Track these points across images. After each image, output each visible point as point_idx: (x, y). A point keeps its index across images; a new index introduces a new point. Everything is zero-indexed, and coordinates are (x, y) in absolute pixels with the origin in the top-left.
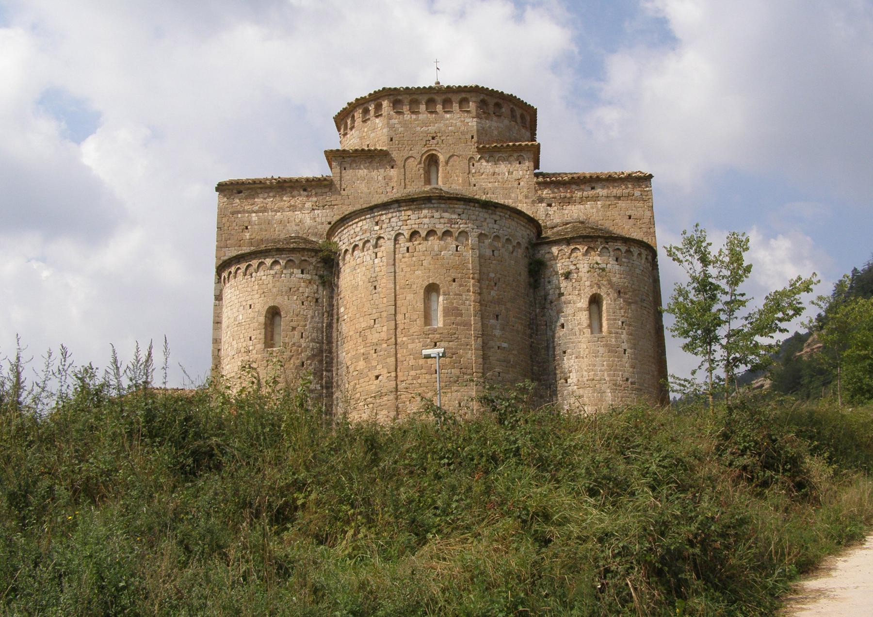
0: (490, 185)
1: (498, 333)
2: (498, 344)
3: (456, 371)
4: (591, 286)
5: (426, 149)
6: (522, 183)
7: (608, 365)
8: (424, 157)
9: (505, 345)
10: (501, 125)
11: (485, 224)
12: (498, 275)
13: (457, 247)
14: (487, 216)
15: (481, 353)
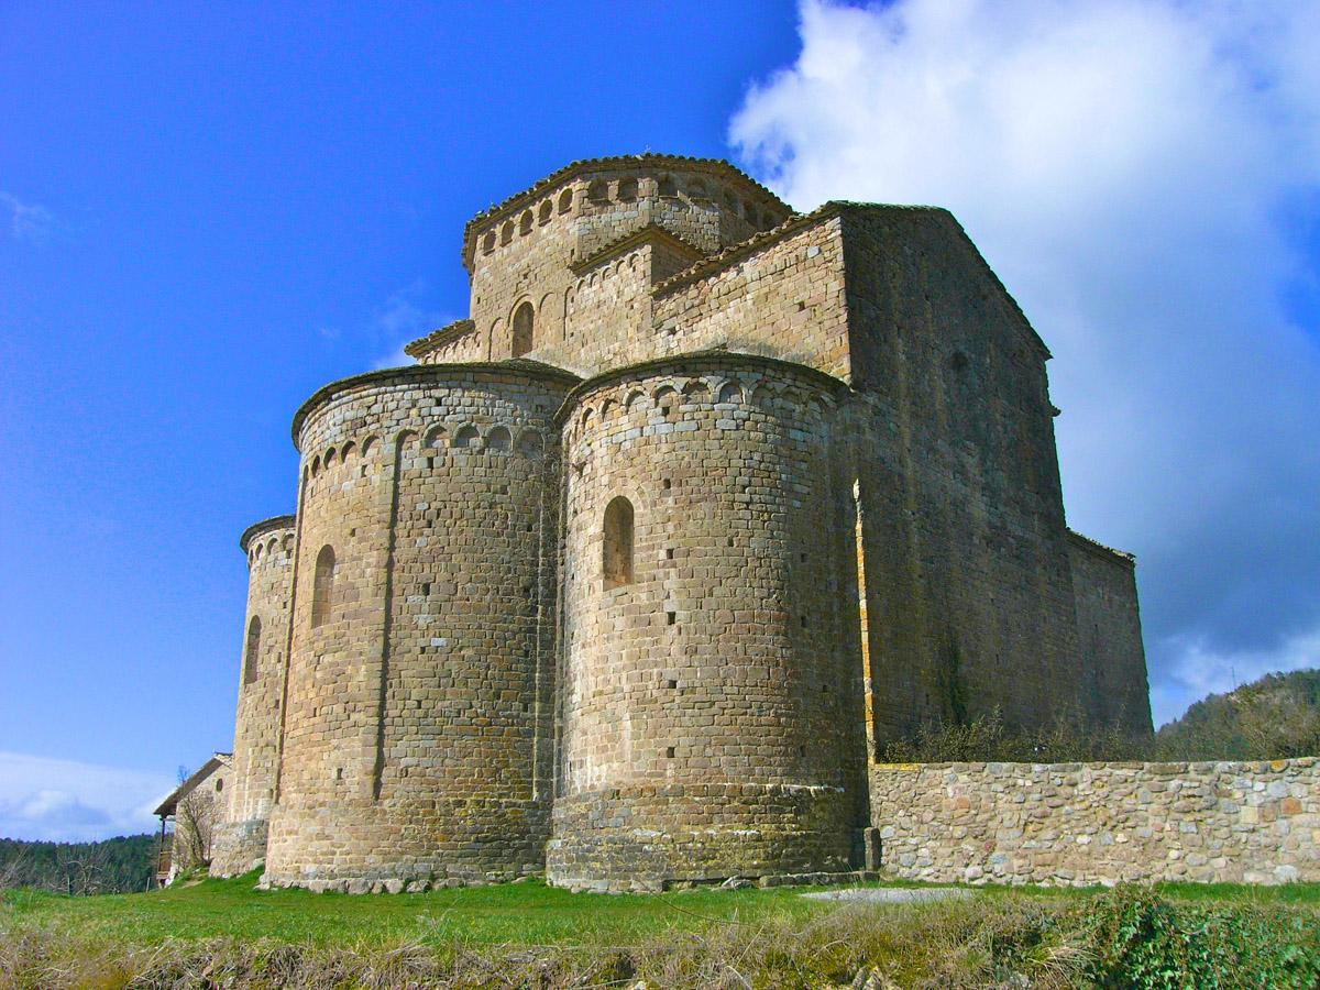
0: (592, 326)
1: (423, 620)
2: (422, 642)
4: (610, 485)
5: (516, 298)
6: (635, 306)
7: (630, 656)
9: (440, 641)
11: (414, 412)
13: (364, 467)
14: (418, 394)
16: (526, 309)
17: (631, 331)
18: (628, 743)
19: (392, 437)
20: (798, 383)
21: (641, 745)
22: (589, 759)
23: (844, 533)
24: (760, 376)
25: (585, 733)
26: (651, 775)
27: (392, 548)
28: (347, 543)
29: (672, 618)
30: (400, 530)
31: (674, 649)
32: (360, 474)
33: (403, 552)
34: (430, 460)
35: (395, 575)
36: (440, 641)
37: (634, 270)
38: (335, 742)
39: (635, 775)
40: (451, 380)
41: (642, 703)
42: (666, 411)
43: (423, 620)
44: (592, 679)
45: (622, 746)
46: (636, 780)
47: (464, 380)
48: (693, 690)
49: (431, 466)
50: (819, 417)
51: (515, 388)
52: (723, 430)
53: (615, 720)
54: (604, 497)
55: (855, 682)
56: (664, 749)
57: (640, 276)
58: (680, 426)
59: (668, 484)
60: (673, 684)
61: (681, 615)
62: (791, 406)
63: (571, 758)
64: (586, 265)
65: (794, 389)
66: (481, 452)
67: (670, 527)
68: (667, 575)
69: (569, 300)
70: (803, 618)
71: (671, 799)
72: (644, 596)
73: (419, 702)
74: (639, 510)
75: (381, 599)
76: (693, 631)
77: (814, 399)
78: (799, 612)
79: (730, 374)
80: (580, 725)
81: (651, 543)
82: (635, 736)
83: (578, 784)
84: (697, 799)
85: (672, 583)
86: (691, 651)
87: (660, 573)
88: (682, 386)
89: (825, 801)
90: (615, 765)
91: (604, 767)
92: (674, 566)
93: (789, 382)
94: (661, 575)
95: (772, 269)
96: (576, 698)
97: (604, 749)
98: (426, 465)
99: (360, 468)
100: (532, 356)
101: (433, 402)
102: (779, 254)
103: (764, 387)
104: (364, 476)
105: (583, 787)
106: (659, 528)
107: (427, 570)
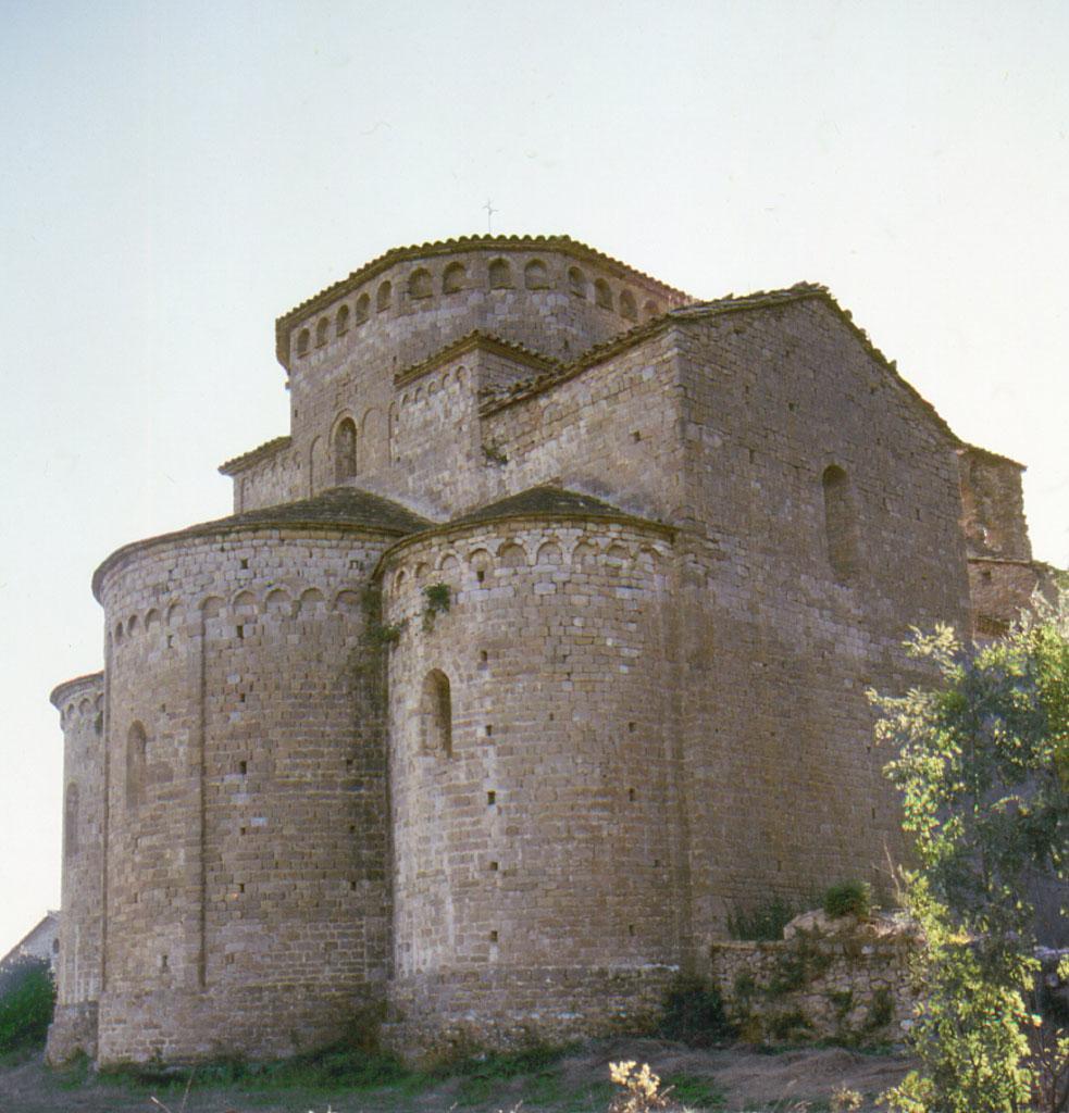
1: (241, 800)
2: (242, 823)
3: (159, 894)
4: (427, 658)
7: (451, 837)
8: (335, 430)
9: (261, 822)
10: (463, 311)
12: (249, 678)
13: (170, 637)
15: (196, 850)
16: (348, 424)
17: (461, 459)
18: (451, 927)
19: (197, 604)
20: (625, 536)
21: (463, 929)
22: (416, 941)
23: (681, 696)
24: (579, 532)
25: (410, 915)
26: (474, 960)
27: (204, 724)
28: (157, 720)
29: (492, 795)
30: (214, 703)
31: (494, 830)
32: (166, 645)
33: (216, 728)
34: (240, 629)
35: (209, 754)
36: (261, 822)
37: (461, 386)
38: (158, 929)
39: (459, 959)
40: (255, 538)
41: (464, 888)
42: (481, 576)
43: (241, 800)
44: (415, 860)
45: (446, 930)
46: (459, 965)
47: (271, 538)
48: (514, 873)
49: (240, 635)
50: (651, 570)
51: (326, 543)
52: (542, 596)
53: (437, 903)
54: (421, 669)
55: (693, 853)
56: (487, 933)
57: (469, 393)
58: (497, 593)
59: (485, 655)
60: (495, 866)
61: (501, 794)
62: (615, 561)
63: (399, 941)
64: (409, 377)
65: (620, 543)
66: (294, 617)
67: (488, 706)
68: (485, 753)
69: (394, 418)
70: (632, 791)
71: (494, 984)
72: (462, 776)
73: (242, 886)
74: (455, 685)
75: (195, 779)
76: (513, 810)
77: (645, 551)
78: (627, 787)
79: (549, 532)
80: (406, 908)
81: (468, 720)
82: (458, 920)
83: (406, 968)
84: (520, 983)
85: (491, 761)
86: (511, 832)
87: (479, 751)
88: (496, 549)
89: (656, 982)
90: (440, 949)
91: (430, 952)
92: (492, 743)
93: (614, 535)
94: (479, 753)
95: (605, 393)
96: (401, 879)
97: (427, 932)
98: (234, 633)
99: (165, 638)
100: (357, 483)
101: (239, 565)
102: (613, 375)
103: (586, 543)
104: (170, 647)
105: (411, 971)
106: (476, 704)
107: (243, 748)
